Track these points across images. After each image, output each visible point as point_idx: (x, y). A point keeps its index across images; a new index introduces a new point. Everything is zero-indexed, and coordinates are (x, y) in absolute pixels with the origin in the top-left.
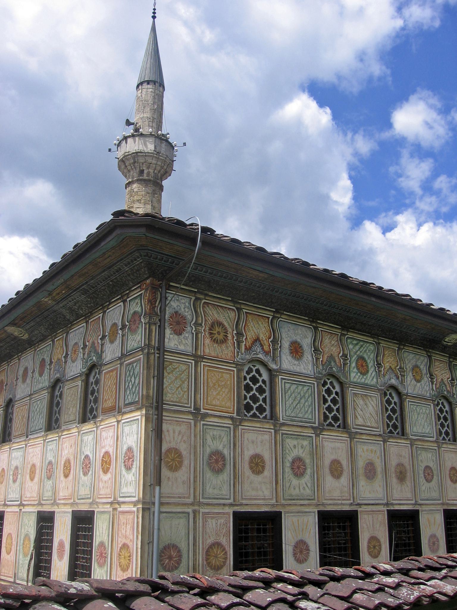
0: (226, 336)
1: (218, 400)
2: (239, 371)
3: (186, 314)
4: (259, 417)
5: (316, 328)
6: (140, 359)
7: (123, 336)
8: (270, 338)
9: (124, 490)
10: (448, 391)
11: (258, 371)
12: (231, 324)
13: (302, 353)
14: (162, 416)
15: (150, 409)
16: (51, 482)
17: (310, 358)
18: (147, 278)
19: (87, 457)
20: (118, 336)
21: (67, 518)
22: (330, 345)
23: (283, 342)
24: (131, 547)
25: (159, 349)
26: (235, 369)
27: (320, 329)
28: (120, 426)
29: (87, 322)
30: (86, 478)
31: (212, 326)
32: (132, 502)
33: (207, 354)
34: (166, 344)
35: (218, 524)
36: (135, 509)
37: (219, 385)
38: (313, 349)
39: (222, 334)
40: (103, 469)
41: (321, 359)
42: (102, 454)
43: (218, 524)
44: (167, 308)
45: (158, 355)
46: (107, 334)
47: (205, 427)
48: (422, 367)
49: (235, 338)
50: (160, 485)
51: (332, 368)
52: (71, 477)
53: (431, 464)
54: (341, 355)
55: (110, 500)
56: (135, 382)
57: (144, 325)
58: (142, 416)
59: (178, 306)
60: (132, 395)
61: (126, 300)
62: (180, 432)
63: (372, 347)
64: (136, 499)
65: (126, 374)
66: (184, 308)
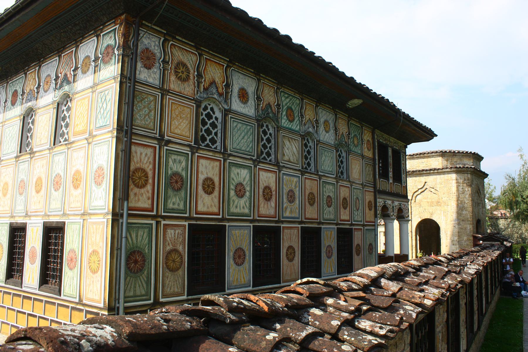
0: (188, 76)
1: (180, 129)
2: (198, 107)
3: (156, 51)
4: (211, 148)
5: (259, 80)
6: (113, 87)
7: (95, 67)
8: (224, 82)
10: (346, 142)
11: (212, 109)
12: (193, 66)
13: (248, 99)
14: (131, 139)
15: (121, 132)
17: (253, 103)
18: (122, 14)
19: (58, 175)
20: (91, 67)
21: (39, 228)
22: (269, 96)
23: (234, 87)
25: (130, 79)
26: (195, 105)
27: (262, 81)
28: (90, 147)
29: (60, 57)
31: (177, 65)
32: (101, 214)
33: (172, 89)
34: (137, 76)
35: (177, 233)
37: (181, 117)
38: (256, 96)
39: (185, 73)
40: (73, 185)
41: (261, 106)
43: (177, 233)
44: (139, 44)
45: (129, 85)
47: (168, 152)
48: (330, 121)
49: (196, 79)
50: (128, 200)
51: (268, 114)
52: (43, 192)
53: (331, 195)
54: (276, 104)
57: (117, 57)
59: (149, 43)
60: (103, 120)
61: (100, 35)
62: (146, 155)
63: (298, 102)
64: (106, 211)
65: (98, 101)
66: (154, 46)
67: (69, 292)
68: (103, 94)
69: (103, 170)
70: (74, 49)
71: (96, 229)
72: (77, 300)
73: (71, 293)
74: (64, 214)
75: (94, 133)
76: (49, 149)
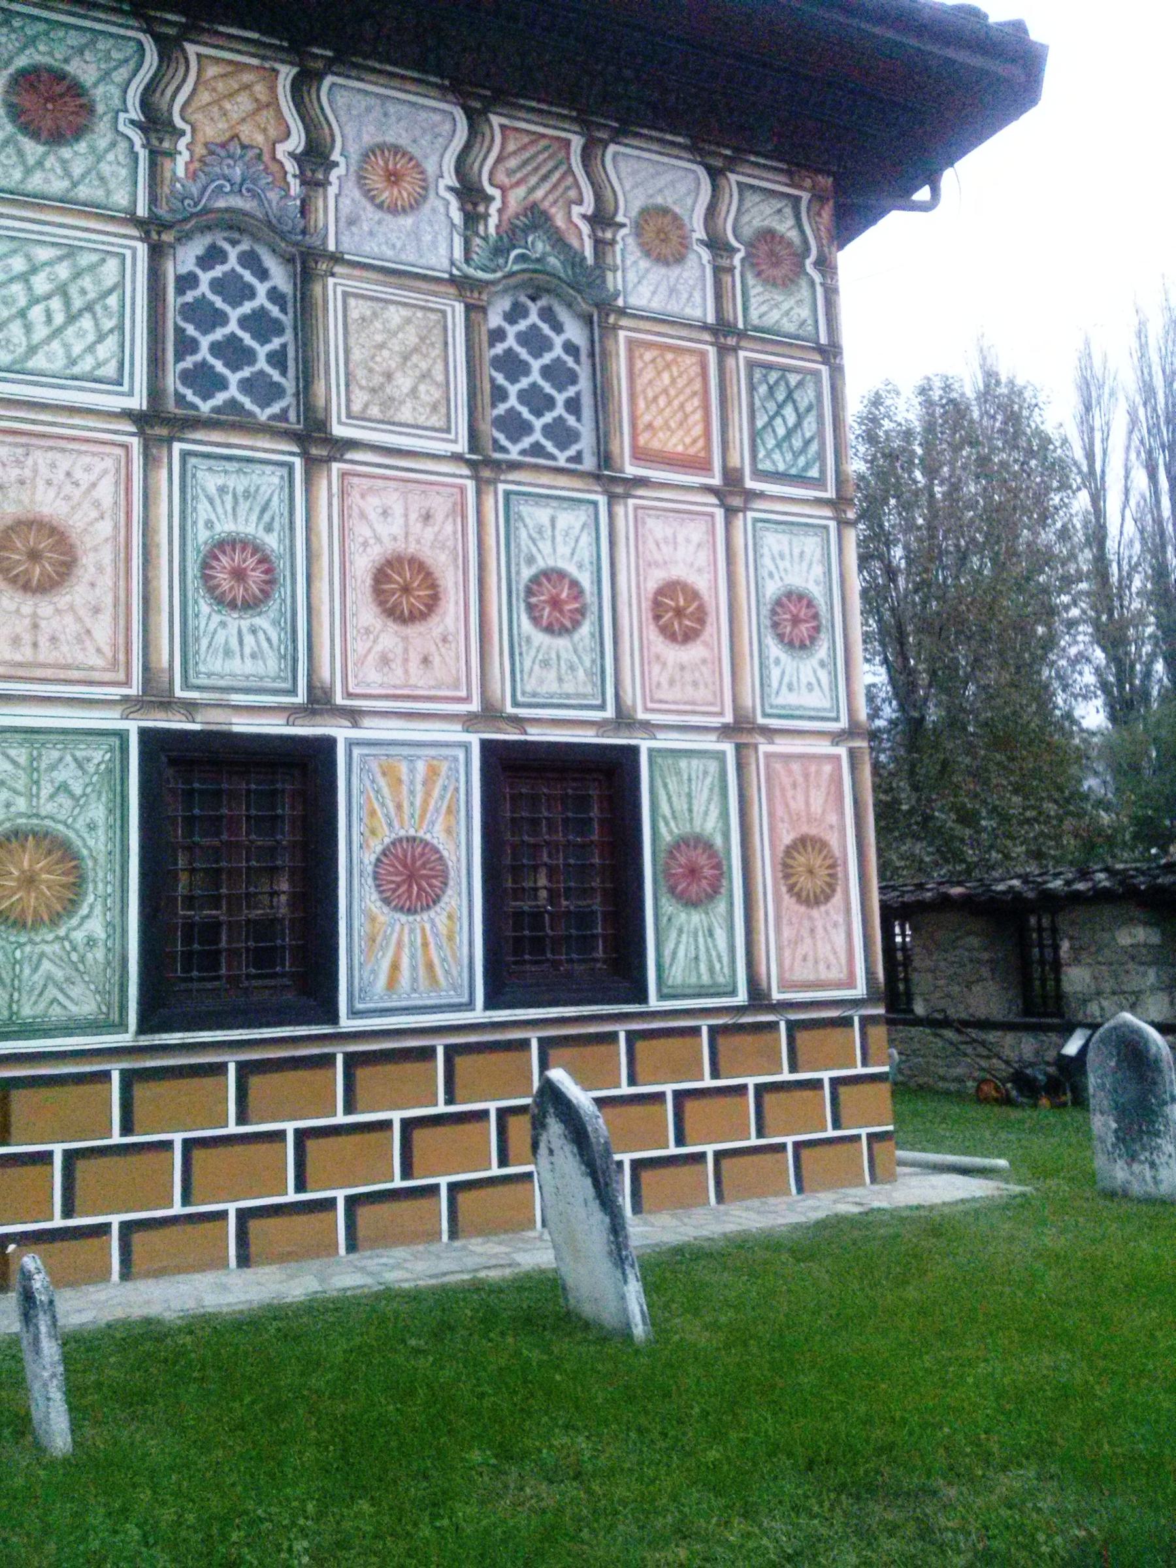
7: (719, 272)
9: (786, 698)
16: (261, 622)
19: (553, 575)
20: (692, 257)
24: (833, 840)
30: (561, 643)
36: (842, 751)
42: (651, 586)
46: (620, 218)
55: (716, 721)
56: (798, 424)
57: (819, 290)
58: (843, 523)
60: (789, 456)
64: (843, 724)
67: (693, 980)
68: (773, 377)
69: (810, 604)
70: (577, 142)
71: (806, 776)
72: (742, 998)
73: (706, 979)
74: (624, 720)
75: (750, 484)
76: (470, 463)
